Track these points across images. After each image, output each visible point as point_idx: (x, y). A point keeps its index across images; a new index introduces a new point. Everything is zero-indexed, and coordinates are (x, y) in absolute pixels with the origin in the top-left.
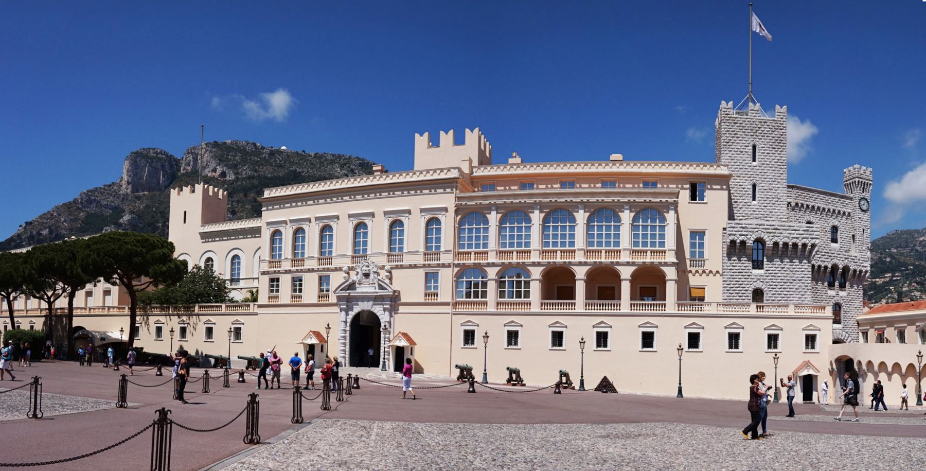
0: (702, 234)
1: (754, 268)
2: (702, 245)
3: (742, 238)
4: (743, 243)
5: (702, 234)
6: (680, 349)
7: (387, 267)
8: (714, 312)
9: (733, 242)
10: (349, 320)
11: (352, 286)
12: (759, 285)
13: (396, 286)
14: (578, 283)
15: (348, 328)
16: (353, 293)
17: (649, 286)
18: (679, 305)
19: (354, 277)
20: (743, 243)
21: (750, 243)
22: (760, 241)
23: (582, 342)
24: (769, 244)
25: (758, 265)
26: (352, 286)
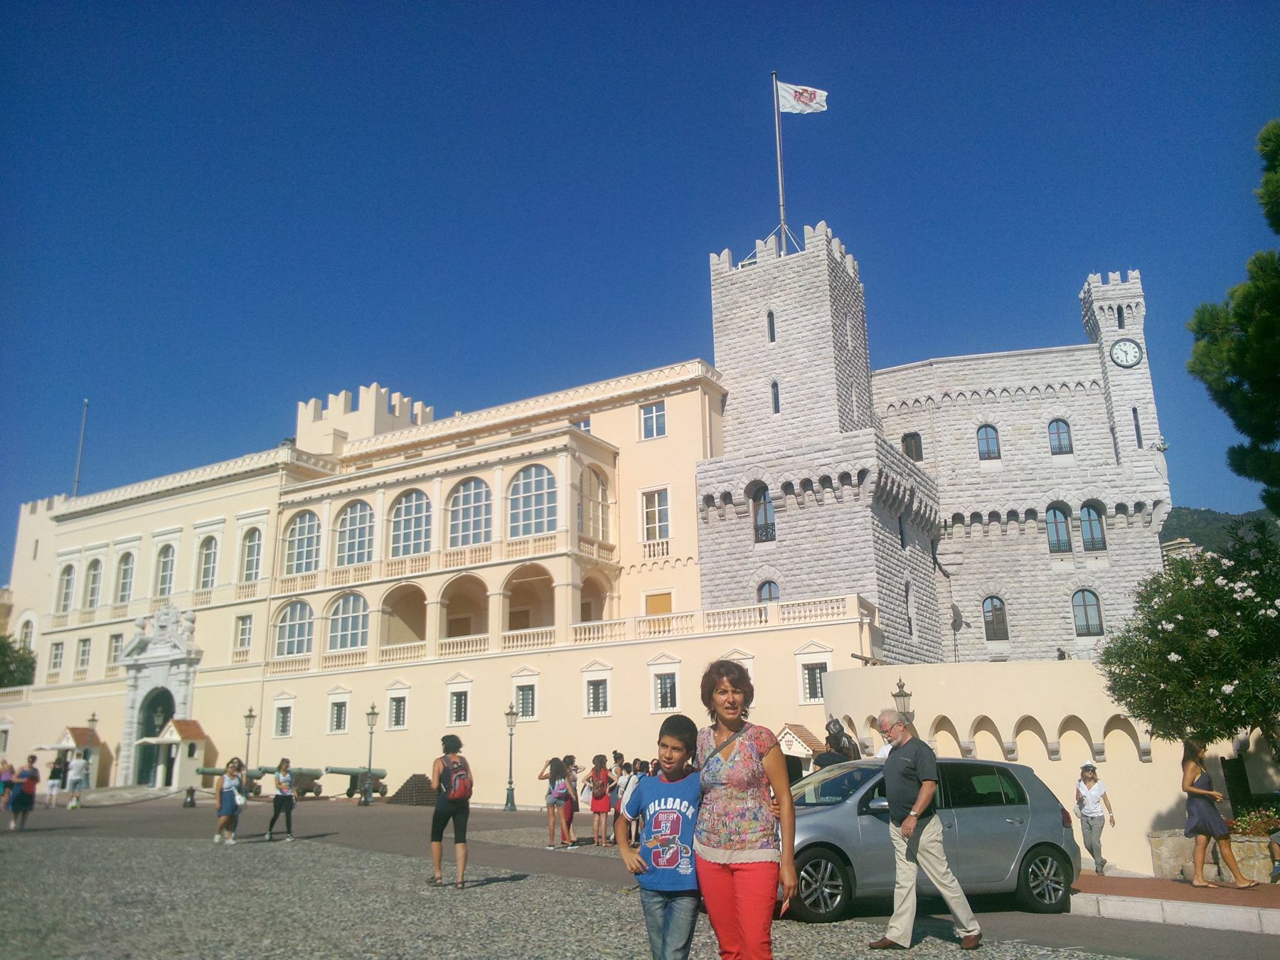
0: (662, 494)
1: (758, 540)
2: (663, 516)
3: (724, 487)
4: (727, 497)
5: (662, 494)
6: (511, 714)
7: (190, 615)
8: (630, 637)
9: (709, 500)
10: (138, 705)
11: (142, 647)
12: (768, 573)
13: (199, 642)
14: (491, 600)
15: (136, 720)
16: (142, 658)
17: (529, 601)
18: (576, 630)
19: (150, 633)
20: (727, 497)
21: (739, 494)
22: (757, 490)
23: (373, 714)
24: (774, 490)
25: (764, 533)
26: (142, 647)
